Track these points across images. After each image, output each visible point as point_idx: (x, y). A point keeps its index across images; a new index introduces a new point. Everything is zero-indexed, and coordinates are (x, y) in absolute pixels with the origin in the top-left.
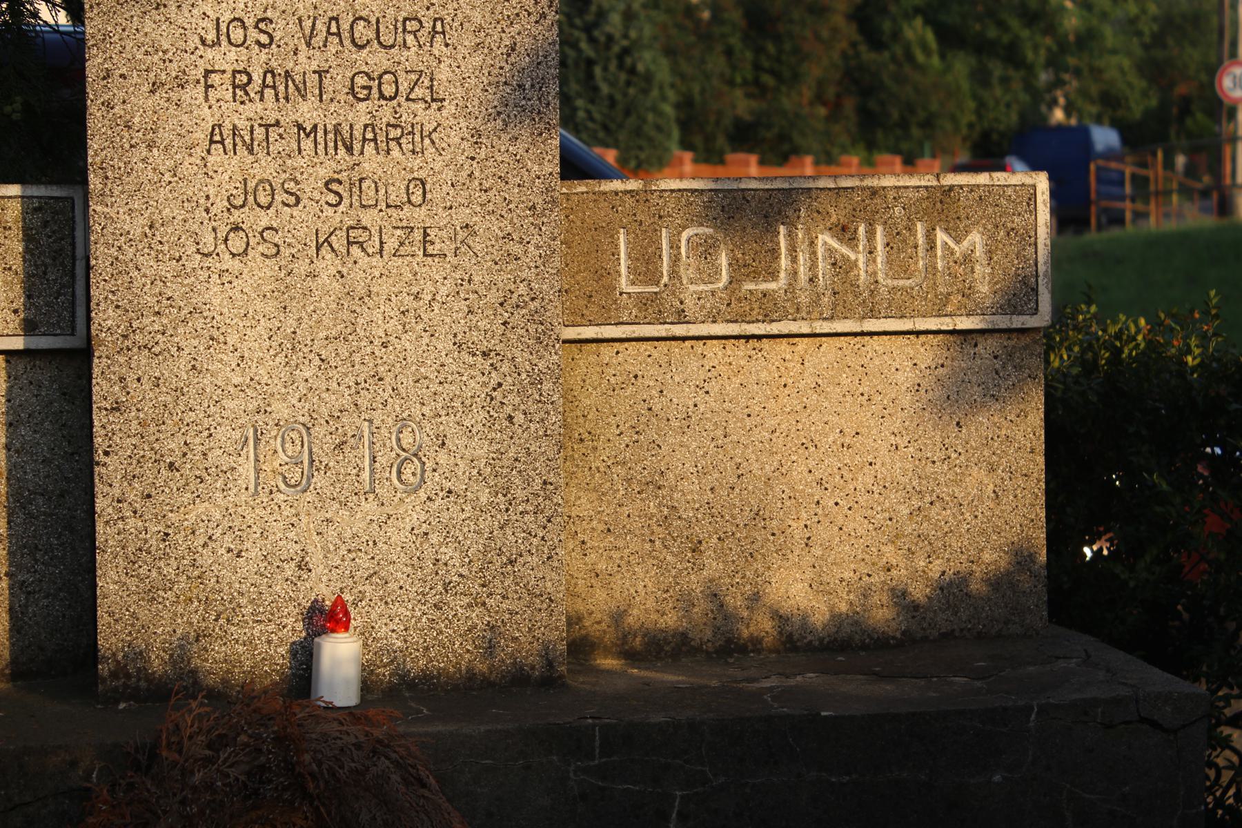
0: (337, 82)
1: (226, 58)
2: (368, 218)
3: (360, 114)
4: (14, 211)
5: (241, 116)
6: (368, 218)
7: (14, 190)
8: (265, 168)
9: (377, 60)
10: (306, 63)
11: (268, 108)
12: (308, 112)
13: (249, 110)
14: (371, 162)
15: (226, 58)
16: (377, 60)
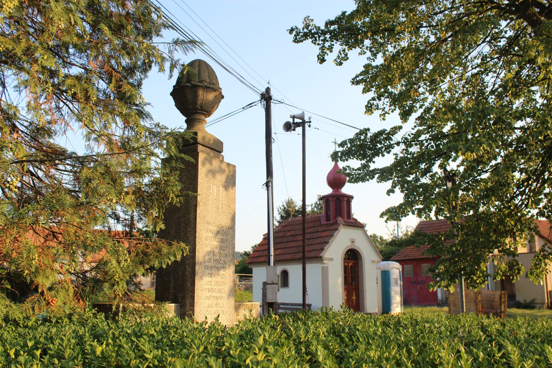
0: (217, 291)
1: (207, 286)
2: (219, 309)
3: (218, 295)
4: (173, 308)
5: (208, 294)
6: (219, 309)
7: (173, 304)
8: (210, 302)
9: (220, 287)
10: (214, 288)
11: (210, 294)
12: (214, 294)
13: (210, 294)
14: (219, 301)
15: (207, 286)
16: (220, 287)
